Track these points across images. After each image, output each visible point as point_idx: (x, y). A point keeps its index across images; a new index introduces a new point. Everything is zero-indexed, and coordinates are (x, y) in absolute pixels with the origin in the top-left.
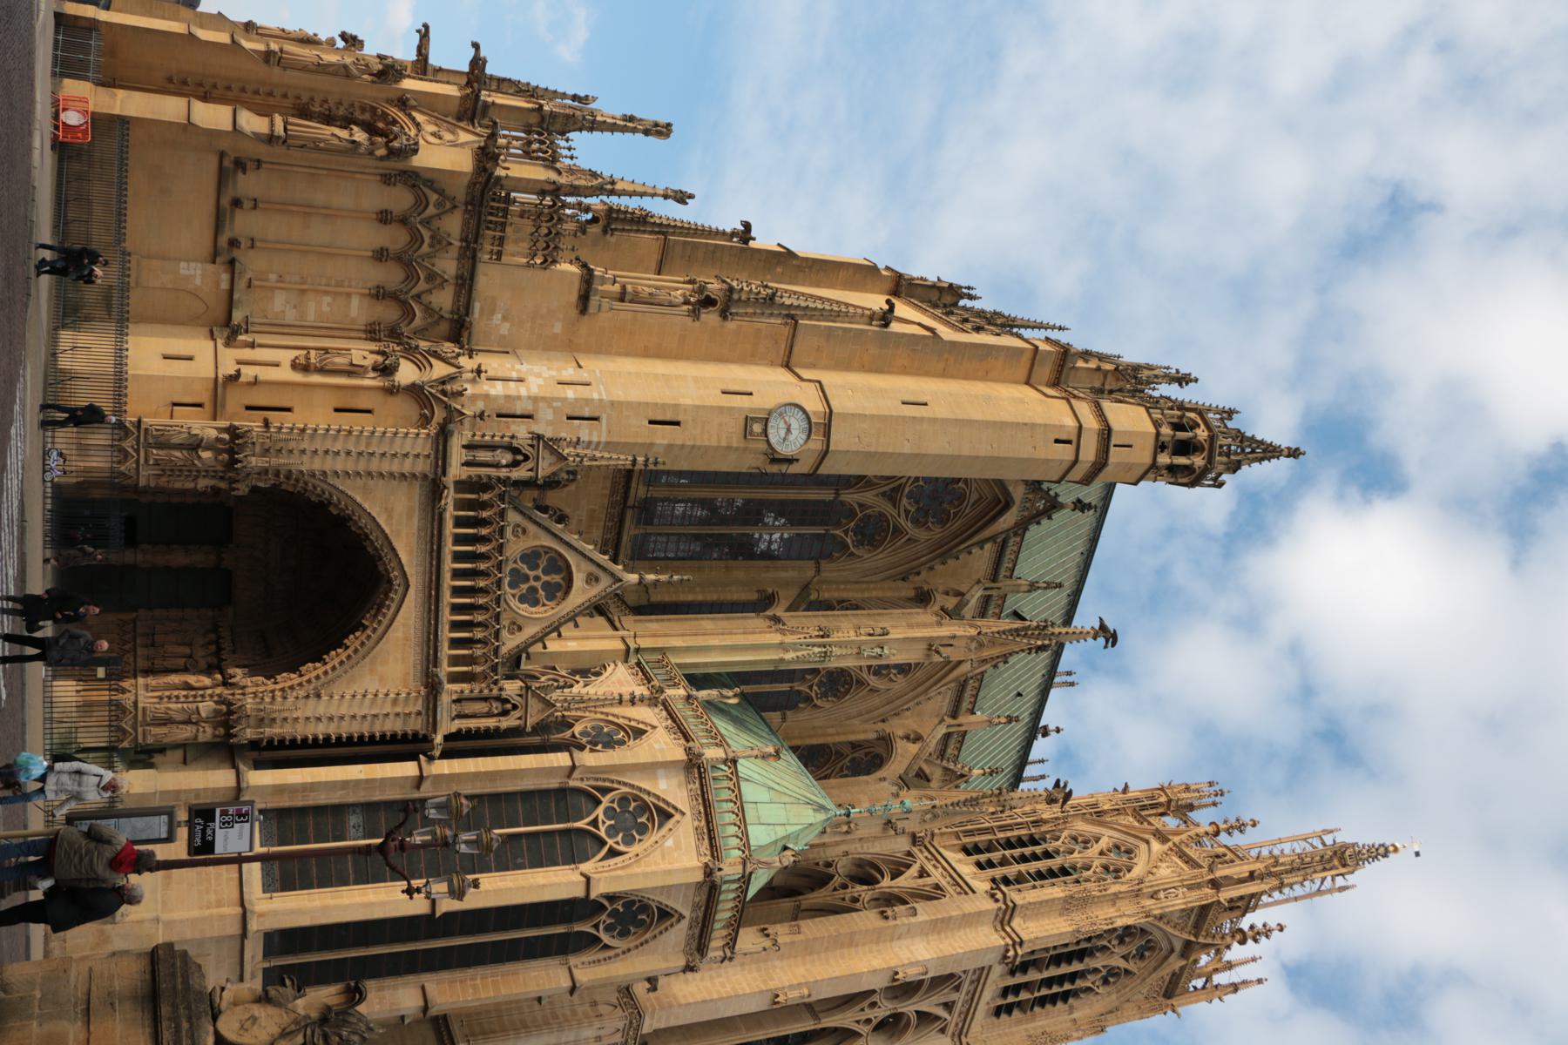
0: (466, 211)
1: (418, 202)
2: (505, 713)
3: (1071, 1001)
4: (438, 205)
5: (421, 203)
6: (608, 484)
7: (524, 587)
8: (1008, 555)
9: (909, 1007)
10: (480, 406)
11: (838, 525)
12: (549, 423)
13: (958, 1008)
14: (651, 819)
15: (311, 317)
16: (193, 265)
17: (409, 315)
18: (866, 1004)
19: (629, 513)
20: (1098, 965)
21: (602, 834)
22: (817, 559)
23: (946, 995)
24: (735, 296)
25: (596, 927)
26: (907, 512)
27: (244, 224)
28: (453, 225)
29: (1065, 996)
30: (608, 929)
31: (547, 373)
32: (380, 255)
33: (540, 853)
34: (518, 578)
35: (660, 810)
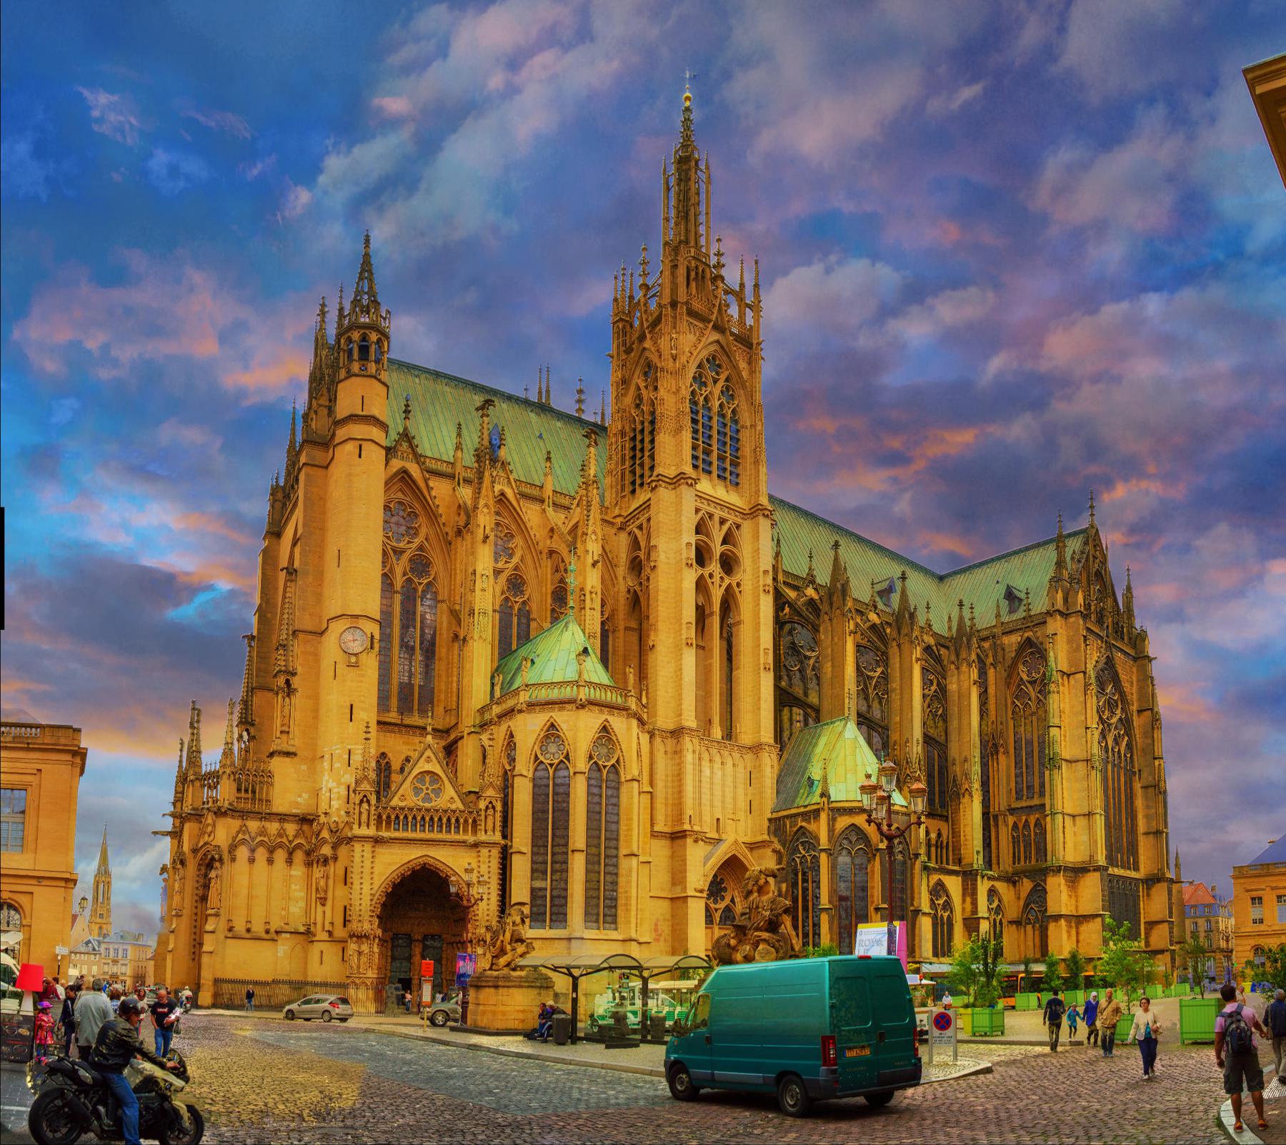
1: (243, 844)
5: (243, 842)
6: (388, 734)
9: (718, 549)
11: (415, 590)
15: (303, 894)
17: (299, 846)
20: (717, 403)
27: (258, 928)
28: (253, 825)
32: (270, 861)
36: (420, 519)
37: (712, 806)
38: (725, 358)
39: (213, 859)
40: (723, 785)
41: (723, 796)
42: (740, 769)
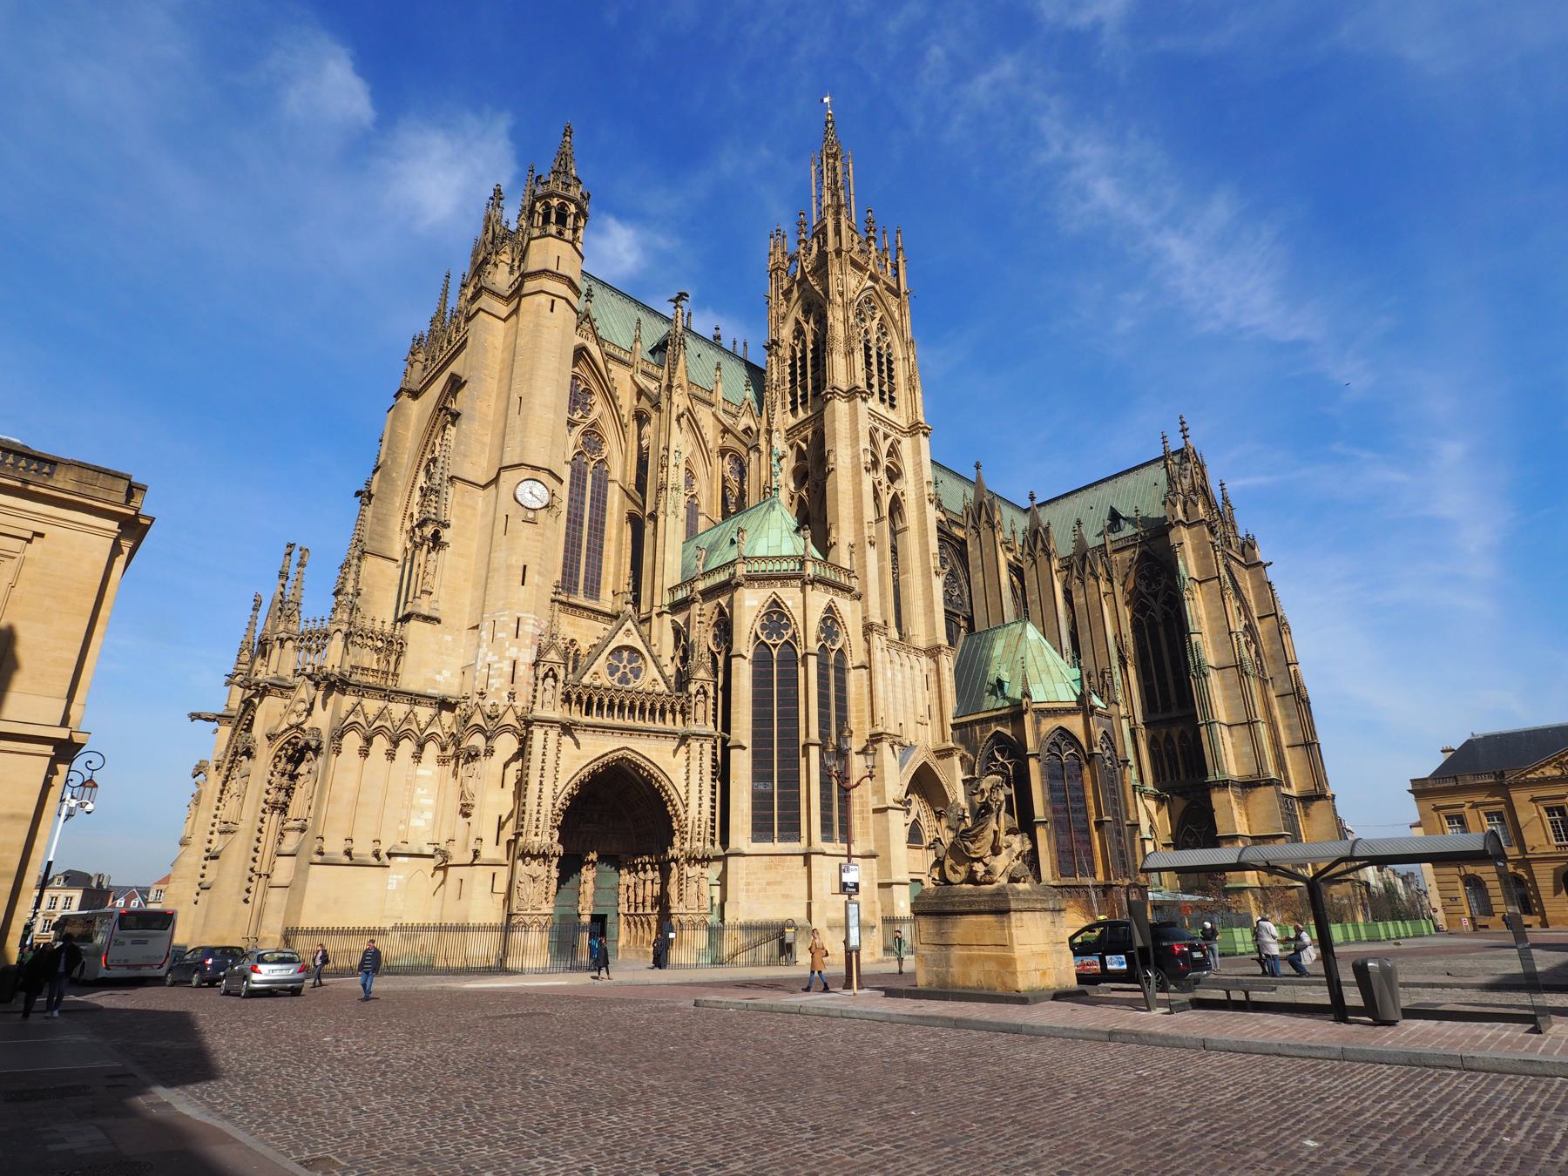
0: (363, 696)
2: (705, 693)
3: (892, 359)
4: (357, 715)
5: (353, 726)
7: (630, 676)
8: (616, 352)
9: (884, 461)
10: (505, 694)
12: (519, 651)
13: (888, 431)
14: (775, 612)
15: (431, 802)
16: (390, 881)
17: (431, 737)
18: (879, 488)
19: (571, 600)
21: (782, 641)
22: (607, 481)
23: (879, 436)
24: (433, 517)
25: (832, 650)
26: (582, 417)
27: (363, 849)
28: (372, 705)
29: (890, 362)
30: (834, 644)
31: (484, 649)
33: (789, 681)
34: (624, 679)
35: (769, 607)
36: (594, 398)
37: (895, 709)
38: (879, 302)
39: (307, 747)
40: (904, 688)
41: (905, 699)
42: (917, 672)
